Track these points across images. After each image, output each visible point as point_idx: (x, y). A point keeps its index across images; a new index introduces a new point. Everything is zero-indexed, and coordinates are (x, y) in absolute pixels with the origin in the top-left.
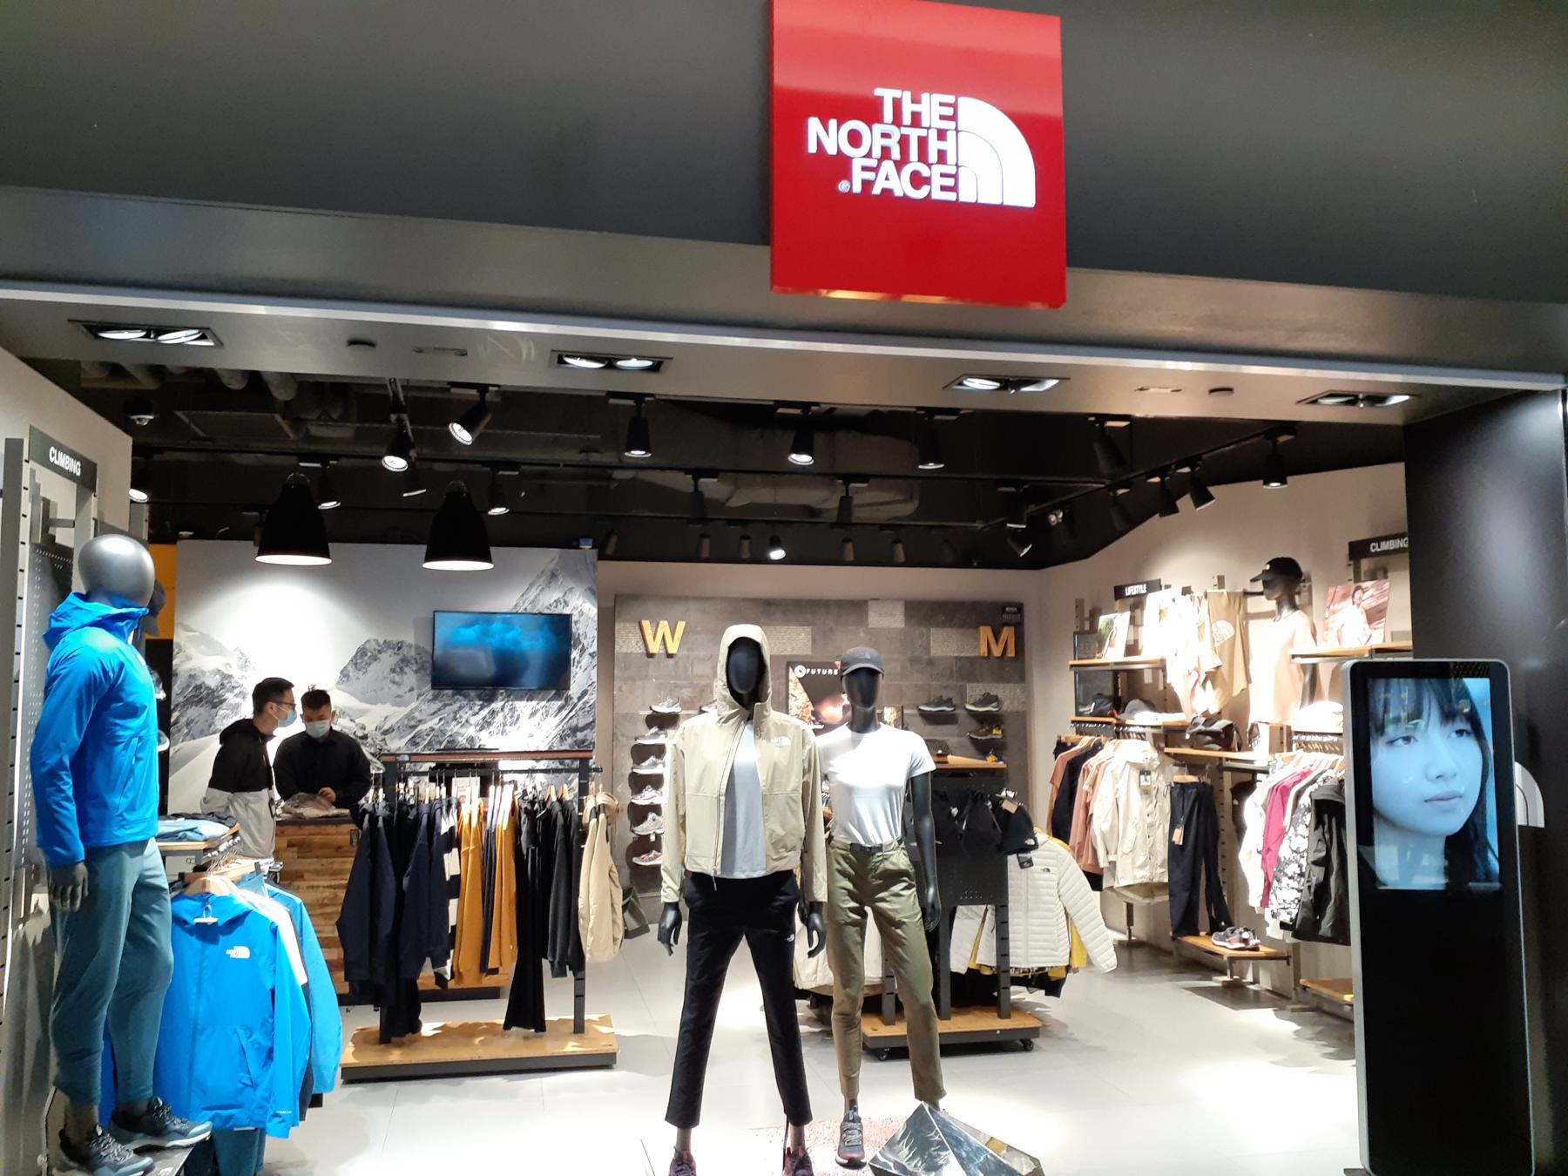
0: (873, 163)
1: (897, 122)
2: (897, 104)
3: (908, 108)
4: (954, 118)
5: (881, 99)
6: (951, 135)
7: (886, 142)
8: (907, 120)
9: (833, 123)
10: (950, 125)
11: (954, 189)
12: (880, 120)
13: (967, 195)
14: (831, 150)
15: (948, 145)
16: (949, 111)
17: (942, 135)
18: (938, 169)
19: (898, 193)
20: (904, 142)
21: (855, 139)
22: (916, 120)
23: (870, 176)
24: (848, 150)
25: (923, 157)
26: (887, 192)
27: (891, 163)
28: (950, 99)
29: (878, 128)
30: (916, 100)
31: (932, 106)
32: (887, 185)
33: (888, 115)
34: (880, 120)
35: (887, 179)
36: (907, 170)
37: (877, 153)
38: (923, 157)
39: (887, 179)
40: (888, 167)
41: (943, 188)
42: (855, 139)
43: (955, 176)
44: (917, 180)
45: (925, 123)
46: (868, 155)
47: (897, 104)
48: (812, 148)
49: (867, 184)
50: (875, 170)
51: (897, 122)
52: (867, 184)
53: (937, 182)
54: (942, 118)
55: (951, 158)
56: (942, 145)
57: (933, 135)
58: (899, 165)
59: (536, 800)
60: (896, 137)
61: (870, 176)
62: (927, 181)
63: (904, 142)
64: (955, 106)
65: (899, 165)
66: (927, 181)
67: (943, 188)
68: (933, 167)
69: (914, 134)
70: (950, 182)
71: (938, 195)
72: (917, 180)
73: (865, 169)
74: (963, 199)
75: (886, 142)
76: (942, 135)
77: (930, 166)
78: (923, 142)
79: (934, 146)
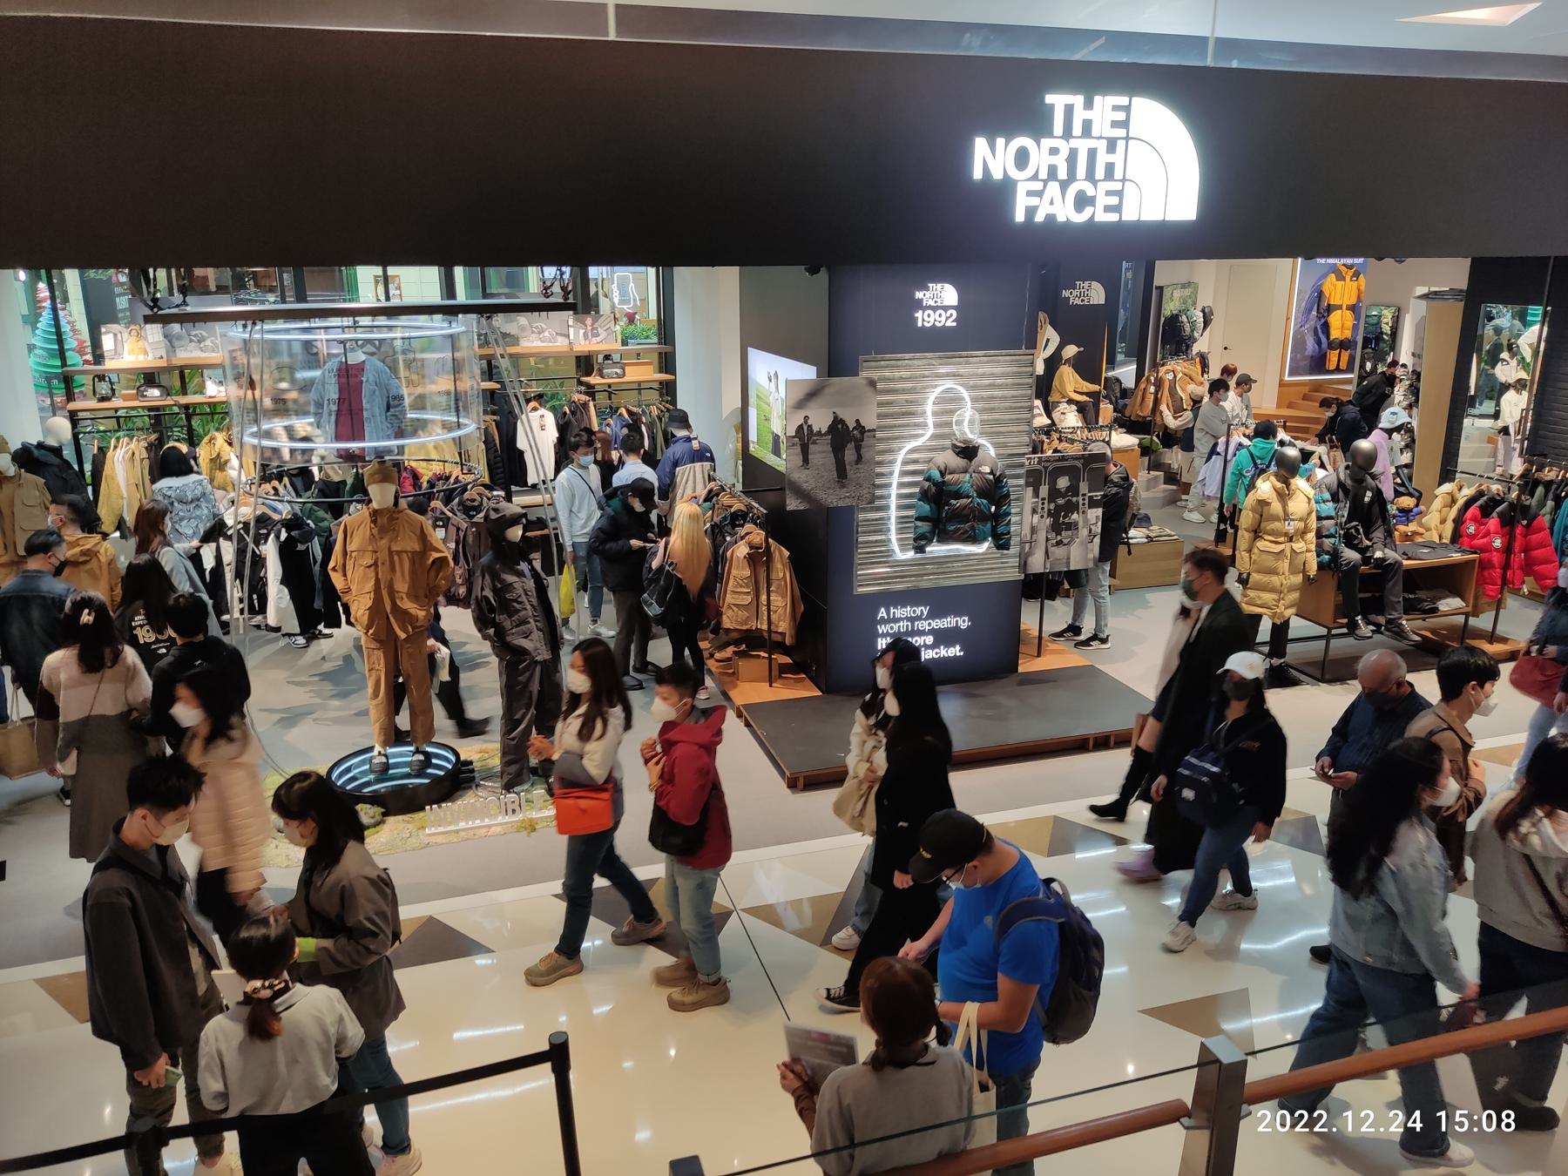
0: (1038, 186)
1: (1068, 134)
2: (1069, 109)
3: (1080, 115)
4: (1125, 124)
5: (1052, 106)
6: (1121, 144)
7: (1054, 160)
8: (1077, 129)
9: (1000, 142)
10: (1121, 133)
11: (1117, 209)
12: (1050, 134)
13: (1130, 214)
14: (997, 175)
15: (1117, 158)
16: (1121, 116)
17: (1112, 145)
18: (1104, 186)
19: (1061, 218)
20: (1073, 154)
21: (1022, 158)
22: (1087, 125)
23: (1034, 201)
24: (1014, 173)
25: (1090, 176)
26: (1050, 218)
27: (1057, 184)
28: (1123, 100)
29: (1046, 143)
30: (1089, 105)
31: (1105, 106)
32: (1051, 210)
33: (1058, 128)
34: (1049, 133)
35: (1052, 203)
36: (1072, 190)
37: (1043, 175)
38: (1090, 176)
39: (1052, 203)
40: (1054, 187)
41: (1108, 209)
42: (1022, 158)
43: (1120, 194)
44: (1082, 201)
45: (1095, 132)
46: (1035, 177)
47: (1069, 109)
48: (978, 174)
49: (1031, 211)
50: (1039, 194)
51: (1068, 134)
52: (1031, 211)
53: (1102, 201)
54: (1115, 124)
55: (1118, 174)
56: (1111, 158)
57: (1102, 146)
58: (1064, 186)
59: (383, 752)
60: (1064, 153)
61: (1034, 201)
62: (1091, 201)
63: (1073, 154)
64: (1127, 109)
65: (1064, 186)
66: (1091, 201)
67: (1108, 209)
68: (1099, 183)
69: (1083, 146)
70: (1114, 201)
71: (1102, 217)
72: (1082, 201)
73: (1030, 194)
74: (1124, 218)
75: (1054, 160)
76: (1112, 145)
77: (1095, 183)
78: (1092, 154)
79: (1102, 158)
